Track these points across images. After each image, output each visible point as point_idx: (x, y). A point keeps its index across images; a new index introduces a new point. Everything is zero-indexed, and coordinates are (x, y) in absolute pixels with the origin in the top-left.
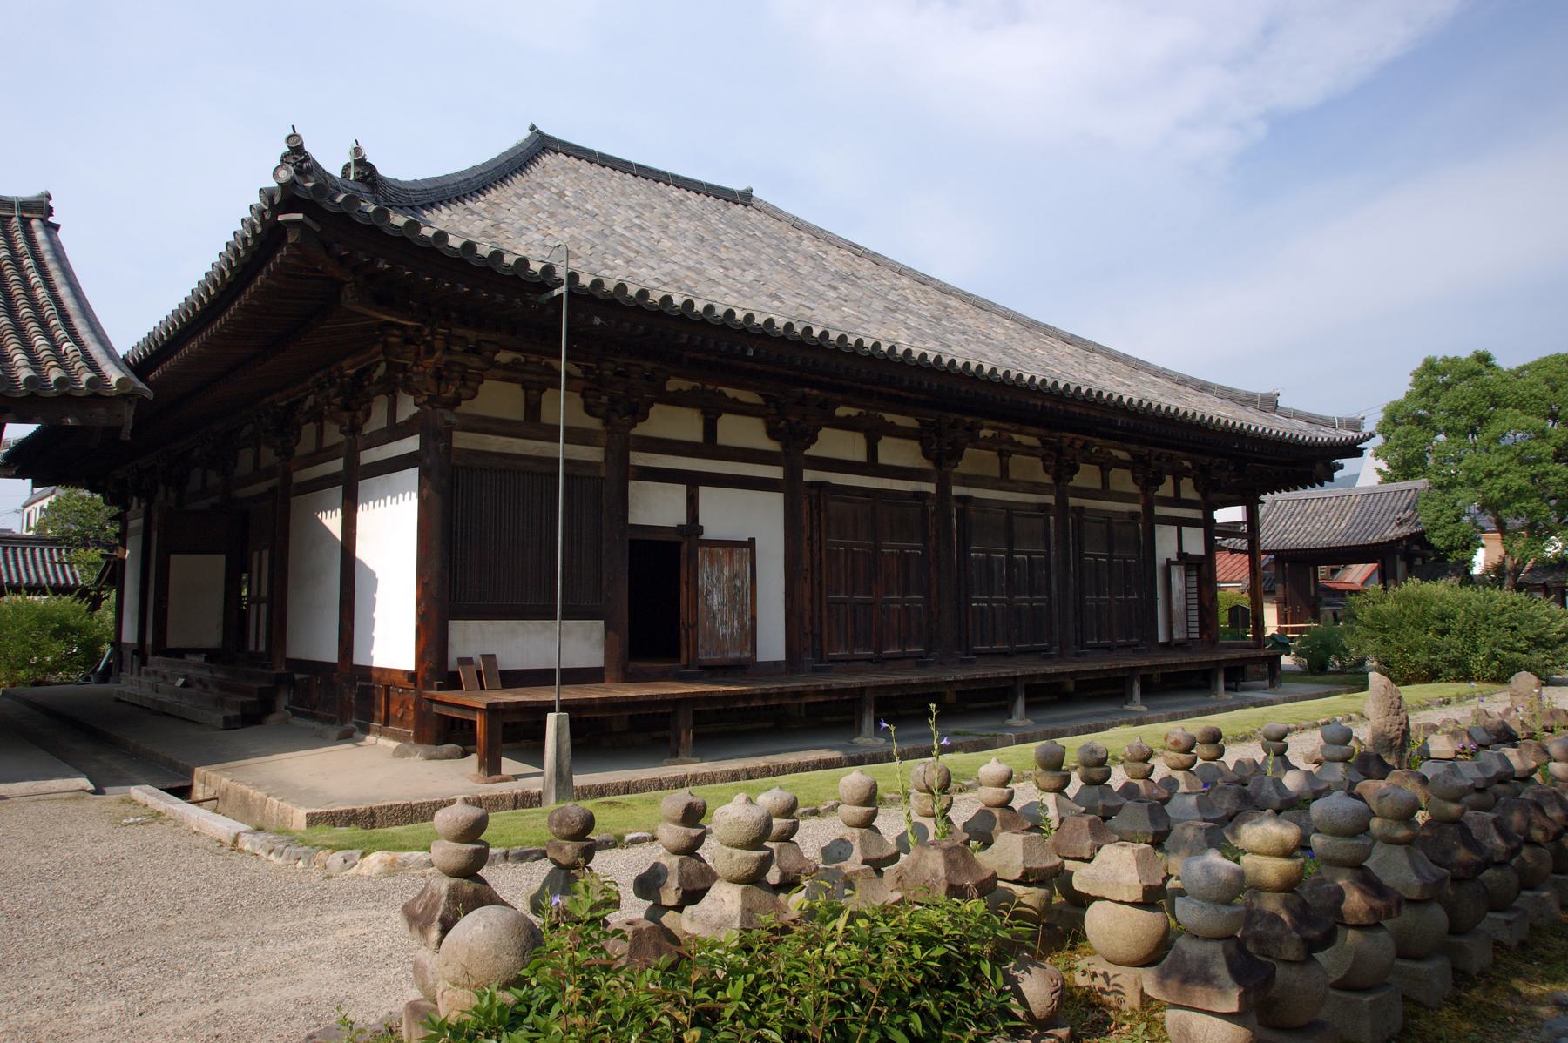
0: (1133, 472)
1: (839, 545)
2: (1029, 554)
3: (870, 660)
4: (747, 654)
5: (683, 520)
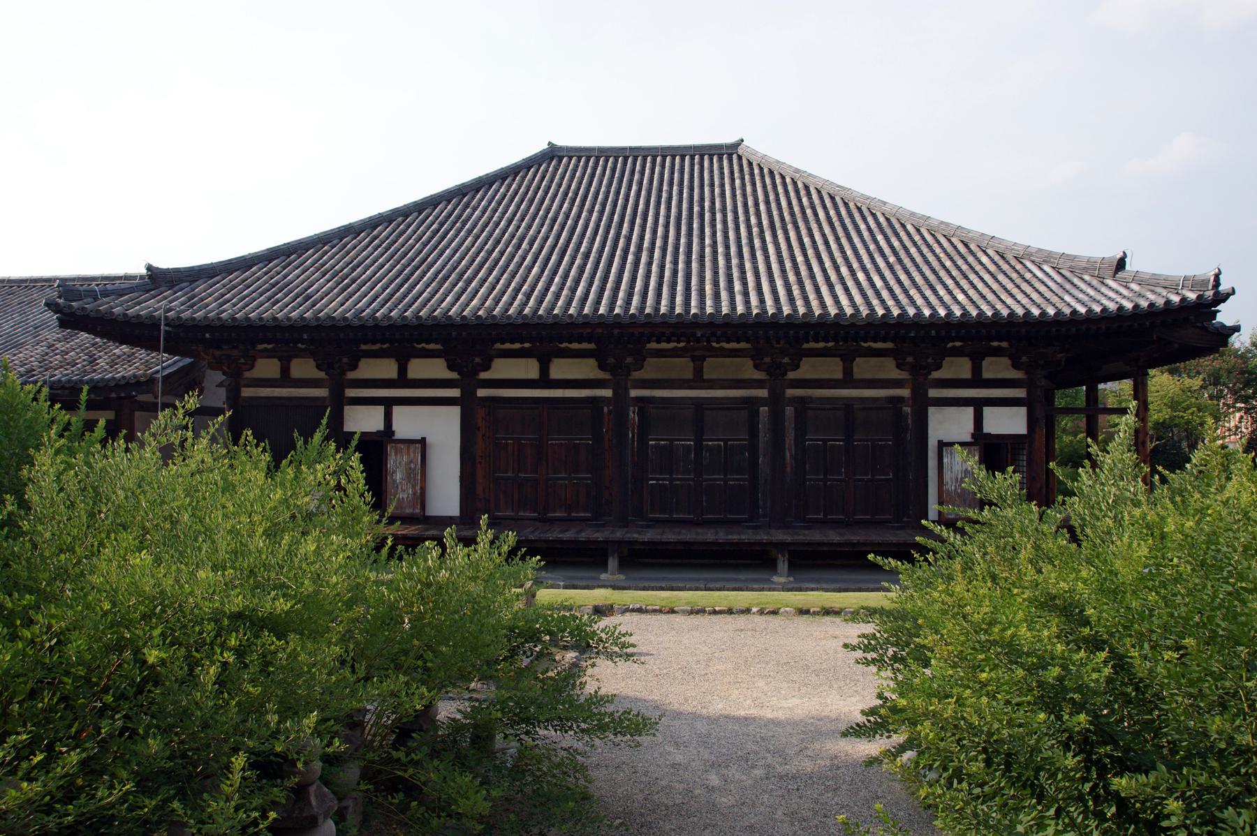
2: (726, 441)
3: (535, 519)
4: (417, 511)
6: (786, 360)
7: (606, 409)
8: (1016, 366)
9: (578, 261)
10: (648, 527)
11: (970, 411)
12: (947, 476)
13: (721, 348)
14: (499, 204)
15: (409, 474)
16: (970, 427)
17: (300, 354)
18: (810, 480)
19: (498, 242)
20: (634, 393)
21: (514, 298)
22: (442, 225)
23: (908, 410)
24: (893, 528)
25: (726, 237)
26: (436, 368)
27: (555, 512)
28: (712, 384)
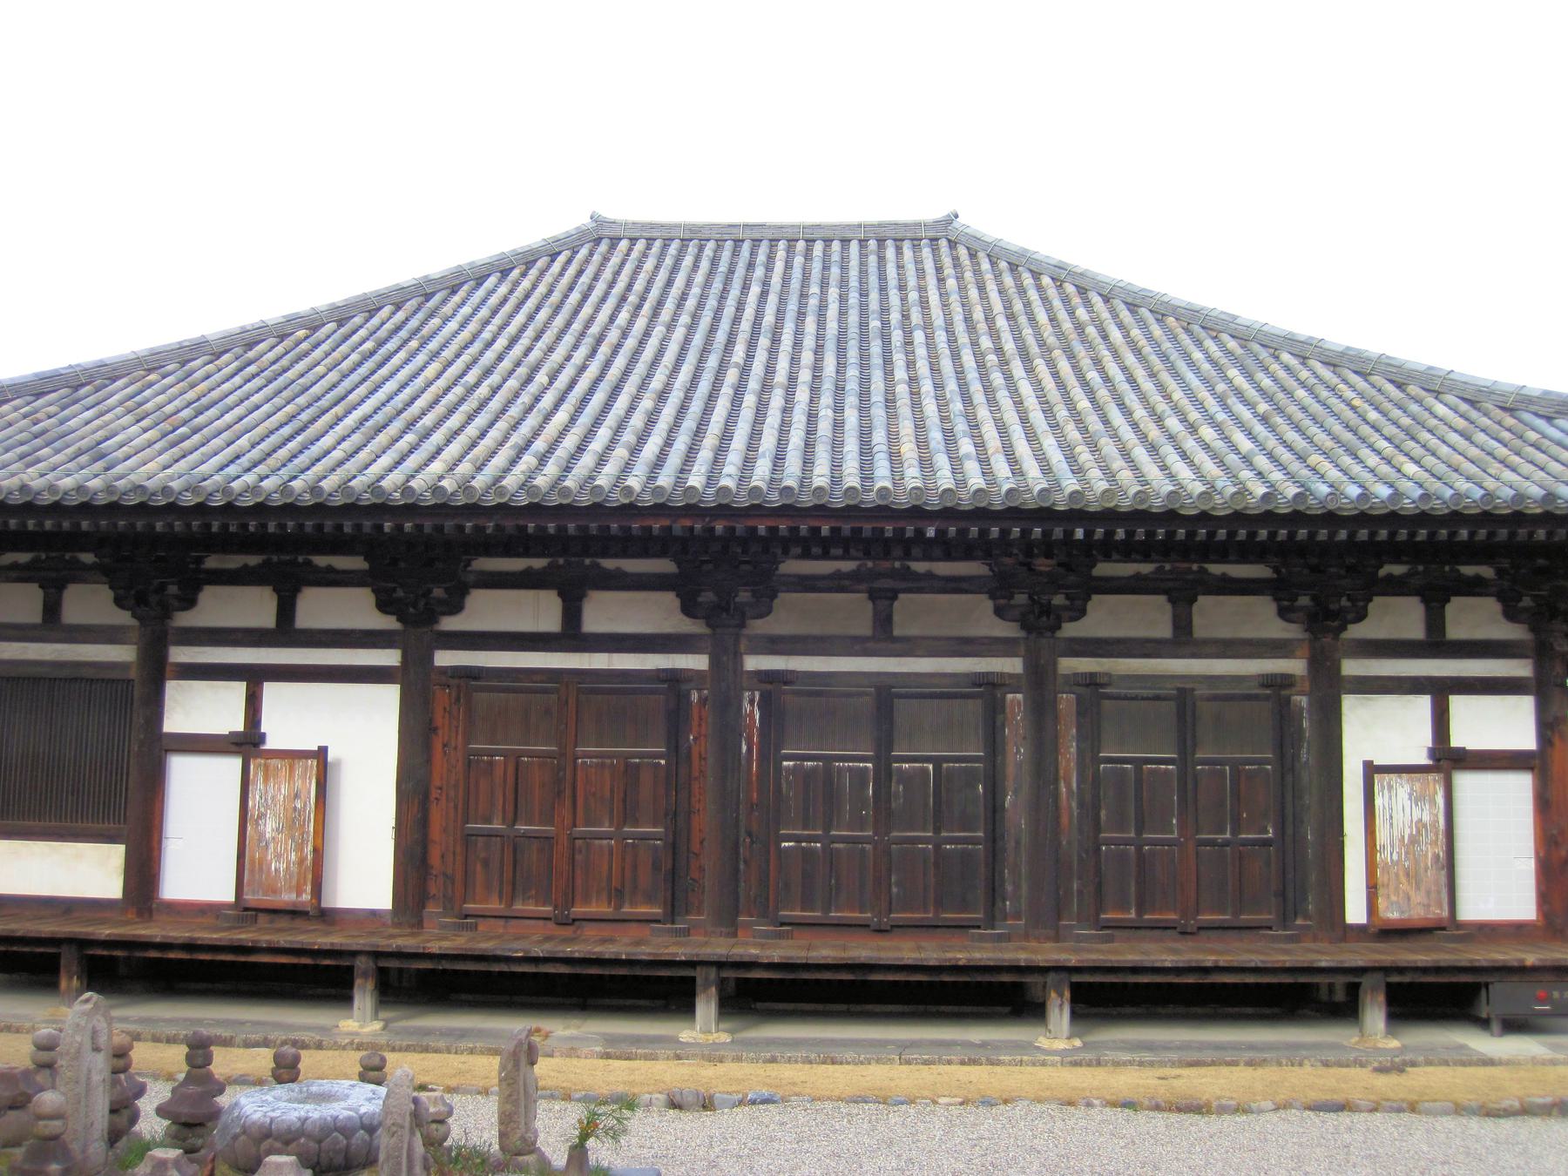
0: (1277, 600)
1: (492, 754)
2: (937, 762)
5: (239, 726)
6: (1059, 600)
7: (695, 696)
8: (1511, 614)
9: (647, 403)
10: (780, 936)
11: (1424, 703)
12: (1382, 836)
13: (930, 575)
14: (495, 312)
15: (292, 823)
16: (1425, 737)
17: (78, 574)
18: (1108, 842)
19: (488, 372)
20: (752, 663)
21: (514, 462)
22: (381, 344)
23: (1303, 701)
24: (1275, 939)
25: (935, 369)
26: (354, 608)
27: (586, 900)
28: (910, 647)
